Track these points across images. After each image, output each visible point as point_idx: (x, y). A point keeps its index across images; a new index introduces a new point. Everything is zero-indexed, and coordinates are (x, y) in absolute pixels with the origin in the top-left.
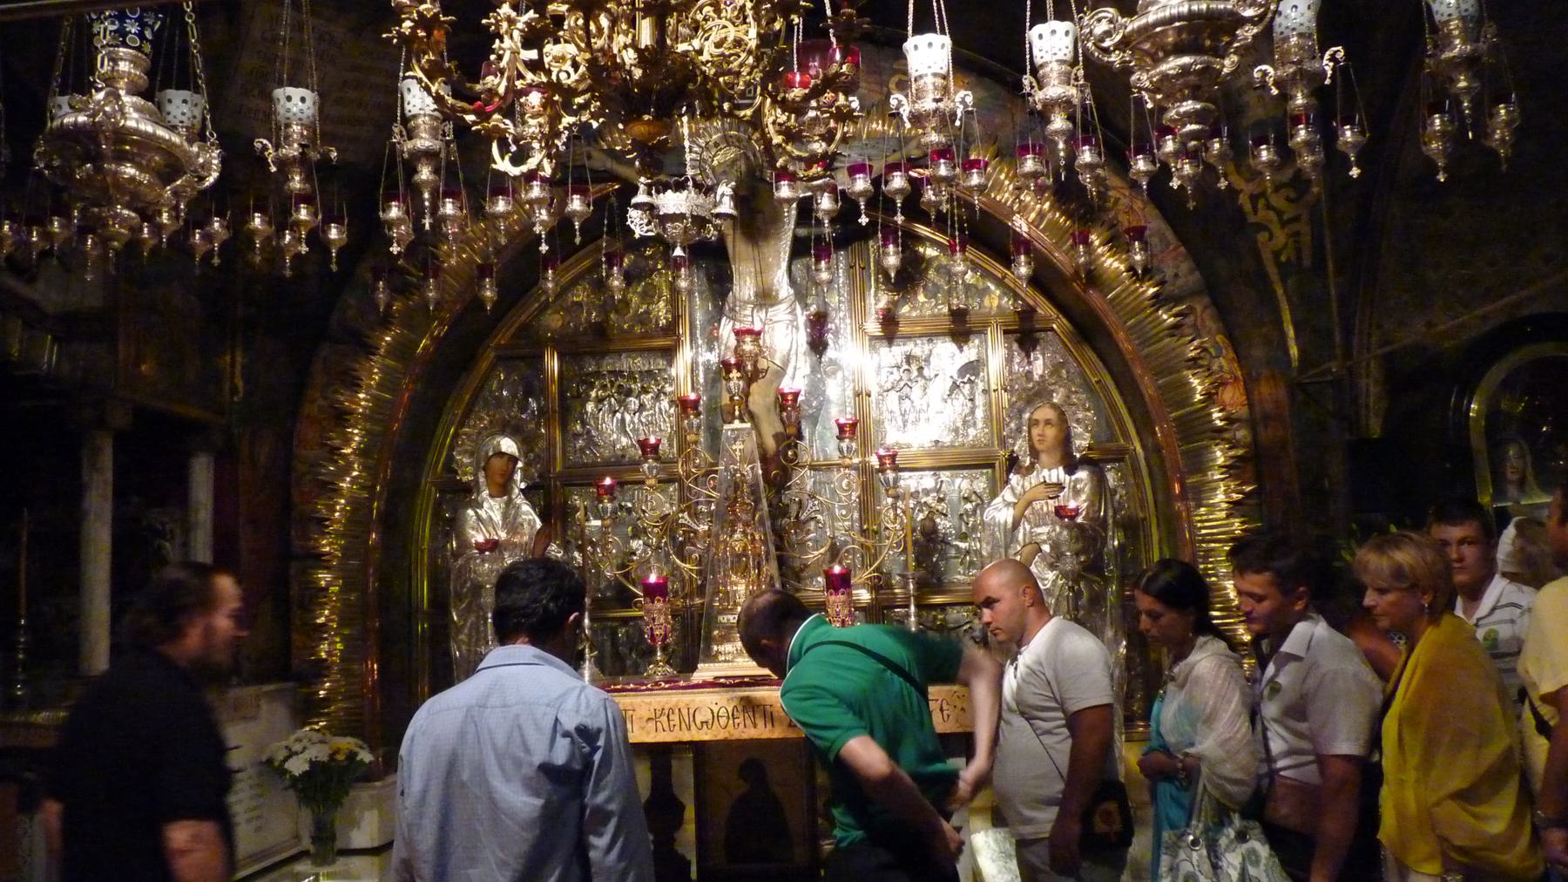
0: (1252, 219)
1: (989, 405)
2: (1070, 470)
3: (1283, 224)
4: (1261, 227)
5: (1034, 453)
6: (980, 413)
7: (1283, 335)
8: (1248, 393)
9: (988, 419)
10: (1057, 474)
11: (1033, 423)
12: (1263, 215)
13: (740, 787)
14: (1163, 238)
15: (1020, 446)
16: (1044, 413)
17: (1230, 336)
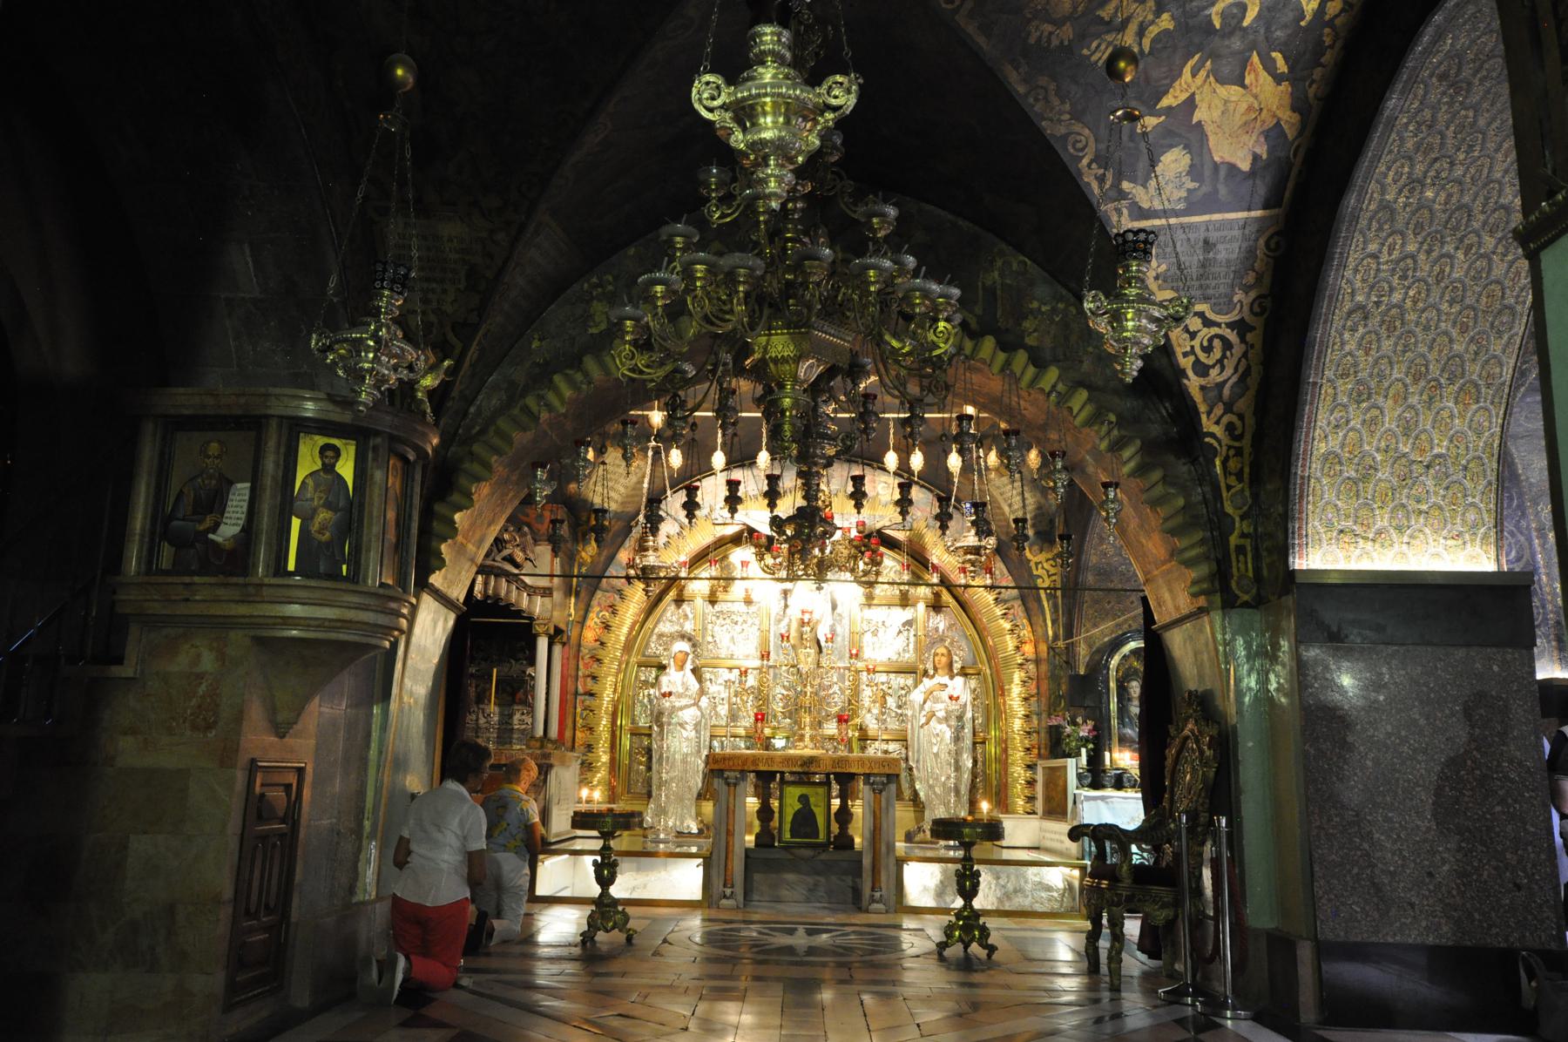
0: (1035, 573)
1: (916, 642)
2: (952, 677)
3: (1049, 576)
4: (1039, 577)
5: (936, 669)
6: (911, 646)
7: (1046, 625)
8: (1036, 647)
9: (916, 649)
10: (945, 680)
11: (936, 655)
12: (1040, 572)
13: (798, 806)
14: (1002, 572)
15: (930, 666)
16: (942, 650)
17: (1030, 621)
